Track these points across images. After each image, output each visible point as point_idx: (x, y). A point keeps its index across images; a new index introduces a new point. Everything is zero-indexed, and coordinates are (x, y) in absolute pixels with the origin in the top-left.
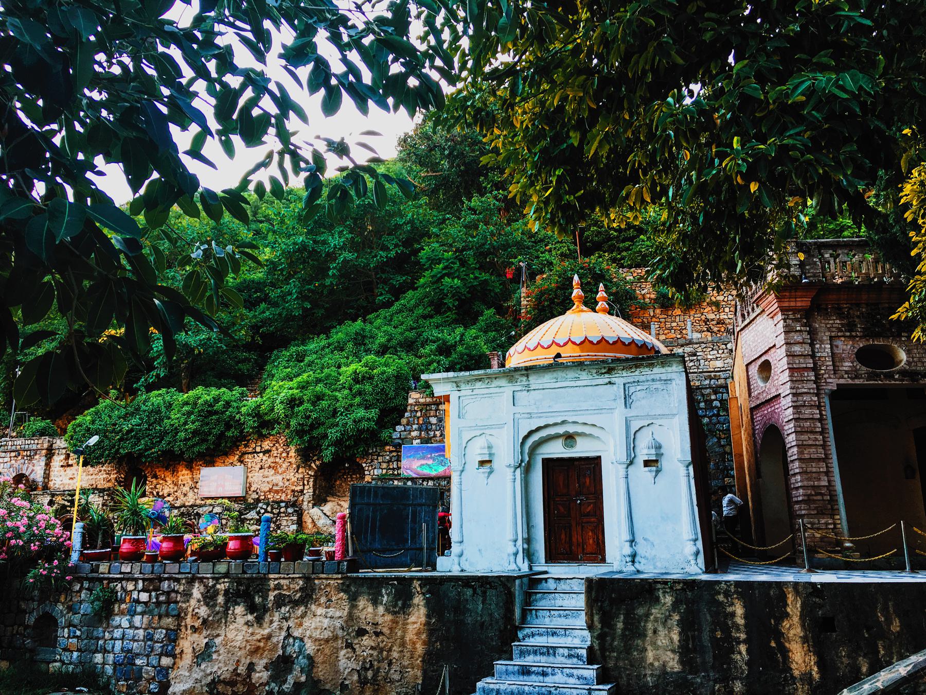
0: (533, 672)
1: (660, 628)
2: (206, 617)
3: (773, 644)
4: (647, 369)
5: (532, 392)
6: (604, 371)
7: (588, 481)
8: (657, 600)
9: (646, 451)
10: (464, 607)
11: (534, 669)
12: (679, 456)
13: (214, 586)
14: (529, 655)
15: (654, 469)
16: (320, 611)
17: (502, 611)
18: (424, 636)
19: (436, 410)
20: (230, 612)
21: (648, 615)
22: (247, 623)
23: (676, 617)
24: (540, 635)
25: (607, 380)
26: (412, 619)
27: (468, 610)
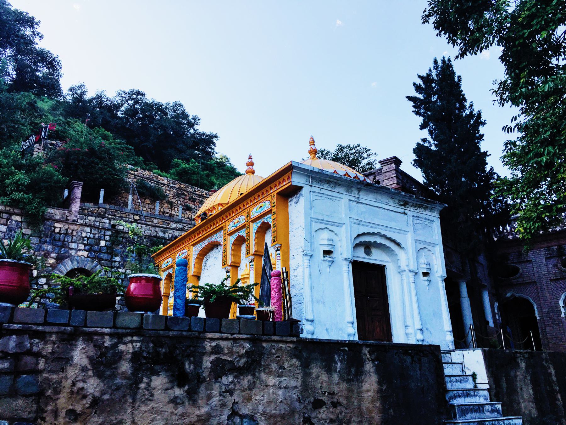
1: (523, 386)
2: (97, 394)
4: (423, 210)
5: (359, 205)
6: (402, 203)
13: (115, 346)
16: (272, 381)
18: (378, 404)
19: (8, 219)
20: (142, 386)
21: (516, 376)
22: (174, 401)
23: (529, 378)
24: (460, 396)
25: (403, 211)
26: (366, 387)
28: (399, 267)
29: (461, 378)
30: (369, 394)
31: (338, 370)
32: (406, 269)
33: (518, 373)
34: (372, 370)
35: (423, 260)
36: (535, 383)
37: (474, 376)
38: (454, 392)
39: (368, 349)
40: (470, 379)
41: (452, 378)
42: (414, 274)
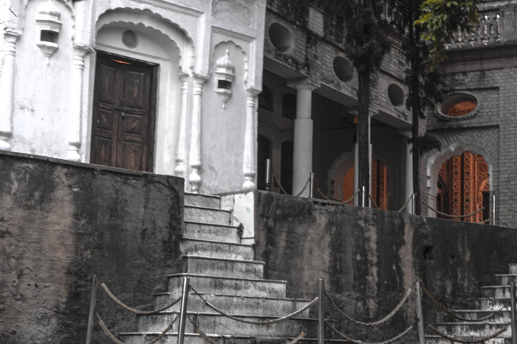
0: (226, 285)
1: (315, 249)
3: (394, 268)
7: (136, 90)
8: (314, 220)
9: (223, 71)
10: (122, 210)
11: (227, 282)
12: (252, 84)
14: (206, 269)
15: (229, 91)
17: (167, 219)
21: (305, 235)
23: (328, 239)
26: (53, 217)
27: (127, 213)
28: (180, 68)
29: (218, 228)
30: (58, 228)
31: (13, 191)
32: (190, 72)
33: (311, 231)
34: (68, 198)
35: (223, 60)
36: (337, 247)
37: (240, 229)
38: (196, 243)
39: (65, 170)
40: (234, 232)
41: (203, 227)
42: (201, 82)
